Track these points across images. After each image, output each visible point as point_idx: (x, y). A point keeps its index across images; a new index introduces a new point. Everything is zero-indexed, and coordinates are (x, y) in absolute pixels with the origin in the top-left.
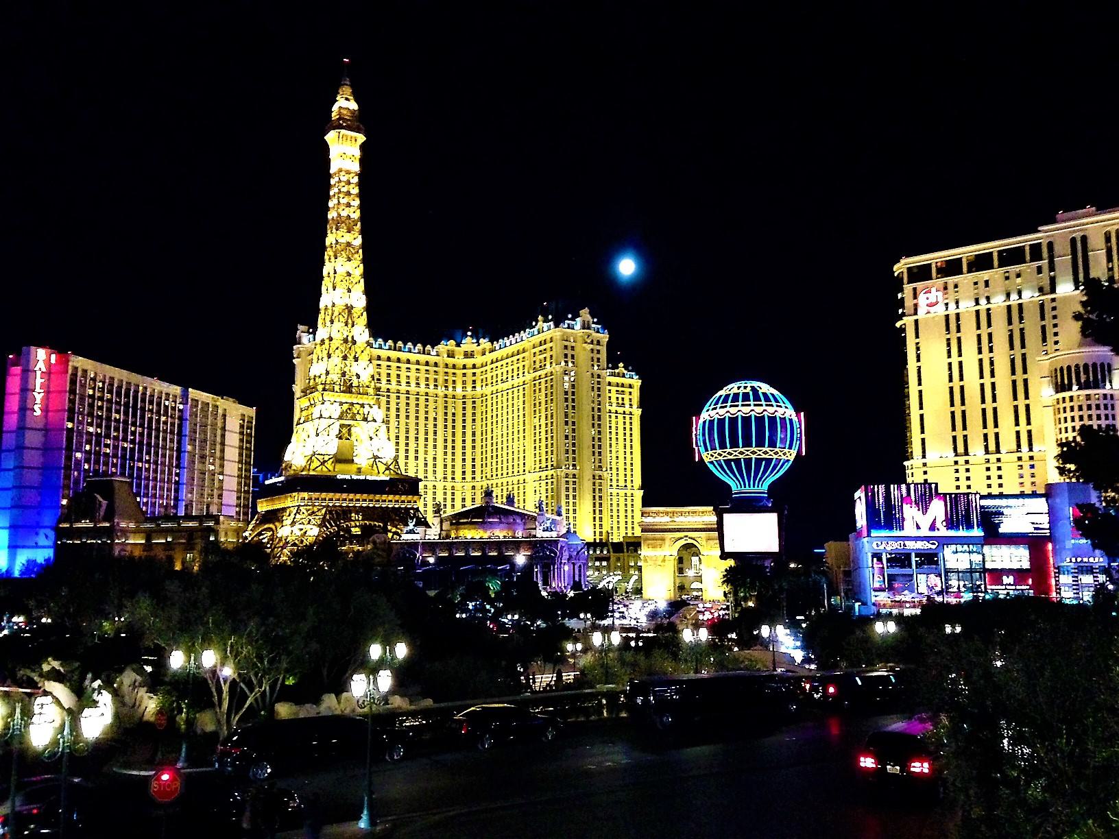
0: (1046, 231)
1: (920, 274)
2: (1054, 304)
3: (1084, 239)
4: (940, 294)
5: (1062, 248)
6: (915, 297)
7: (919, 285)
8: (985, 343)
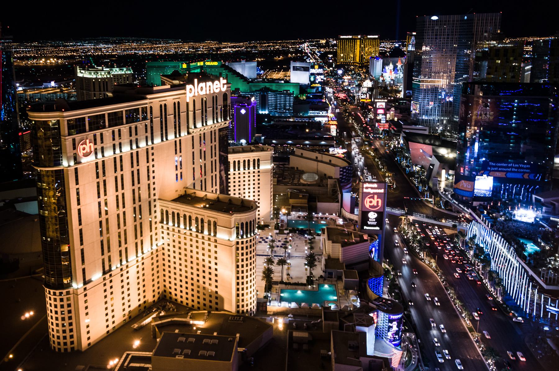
0: (150, 99)
2: (152, 151)
3: (165, 105)
4: (92, 145)
5: (156, 112)
6: (74, 148)
7: (78, 137)
8: (119, 183)
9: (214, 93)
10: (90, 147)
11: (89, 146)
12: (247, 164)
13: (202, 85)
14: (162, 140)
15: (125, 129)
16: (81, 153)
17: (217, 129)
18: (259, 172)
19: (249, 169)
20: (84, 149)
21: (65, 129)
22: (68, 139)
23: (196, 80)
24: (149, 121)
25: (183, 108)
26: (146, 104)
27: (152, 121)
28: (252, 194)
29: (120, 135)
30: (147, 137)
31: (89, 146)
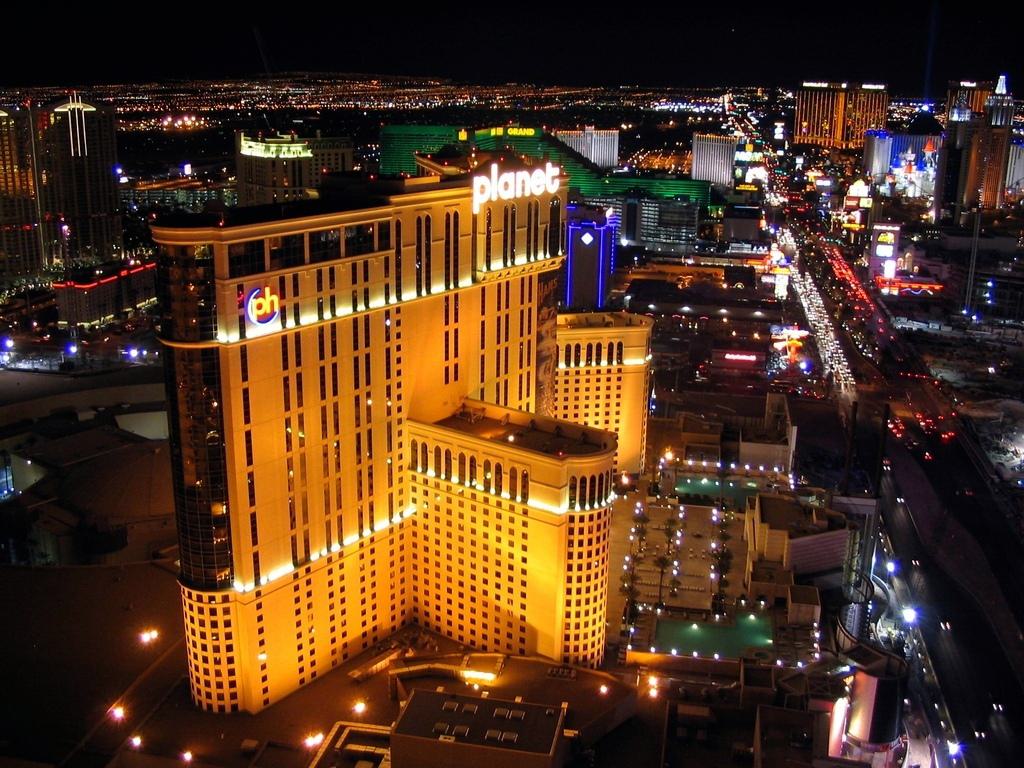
1: (248, 261)
4: (275, 298)
5: (409, 233)
7: (248, 281)
9: (532, 195)
10: (272, 303)
11: (270, 301)
12: (594, 352)
13: (508, 176)
14: (419, 293)
15: (343, 266)
16: (253, 313)
17: (535, 274)
18: (620, 371)
19: (598, 363)
20: (260, 307)
21: (223, 265)
22: (229, 284)
23: (494, 167)
24: (394, 251)
25: (465, 226)
26: (388, 215)
27: (398, 252)
28: (601, 418)
29: (332, 279)
30: (387, 287)
31: (270, 301)
